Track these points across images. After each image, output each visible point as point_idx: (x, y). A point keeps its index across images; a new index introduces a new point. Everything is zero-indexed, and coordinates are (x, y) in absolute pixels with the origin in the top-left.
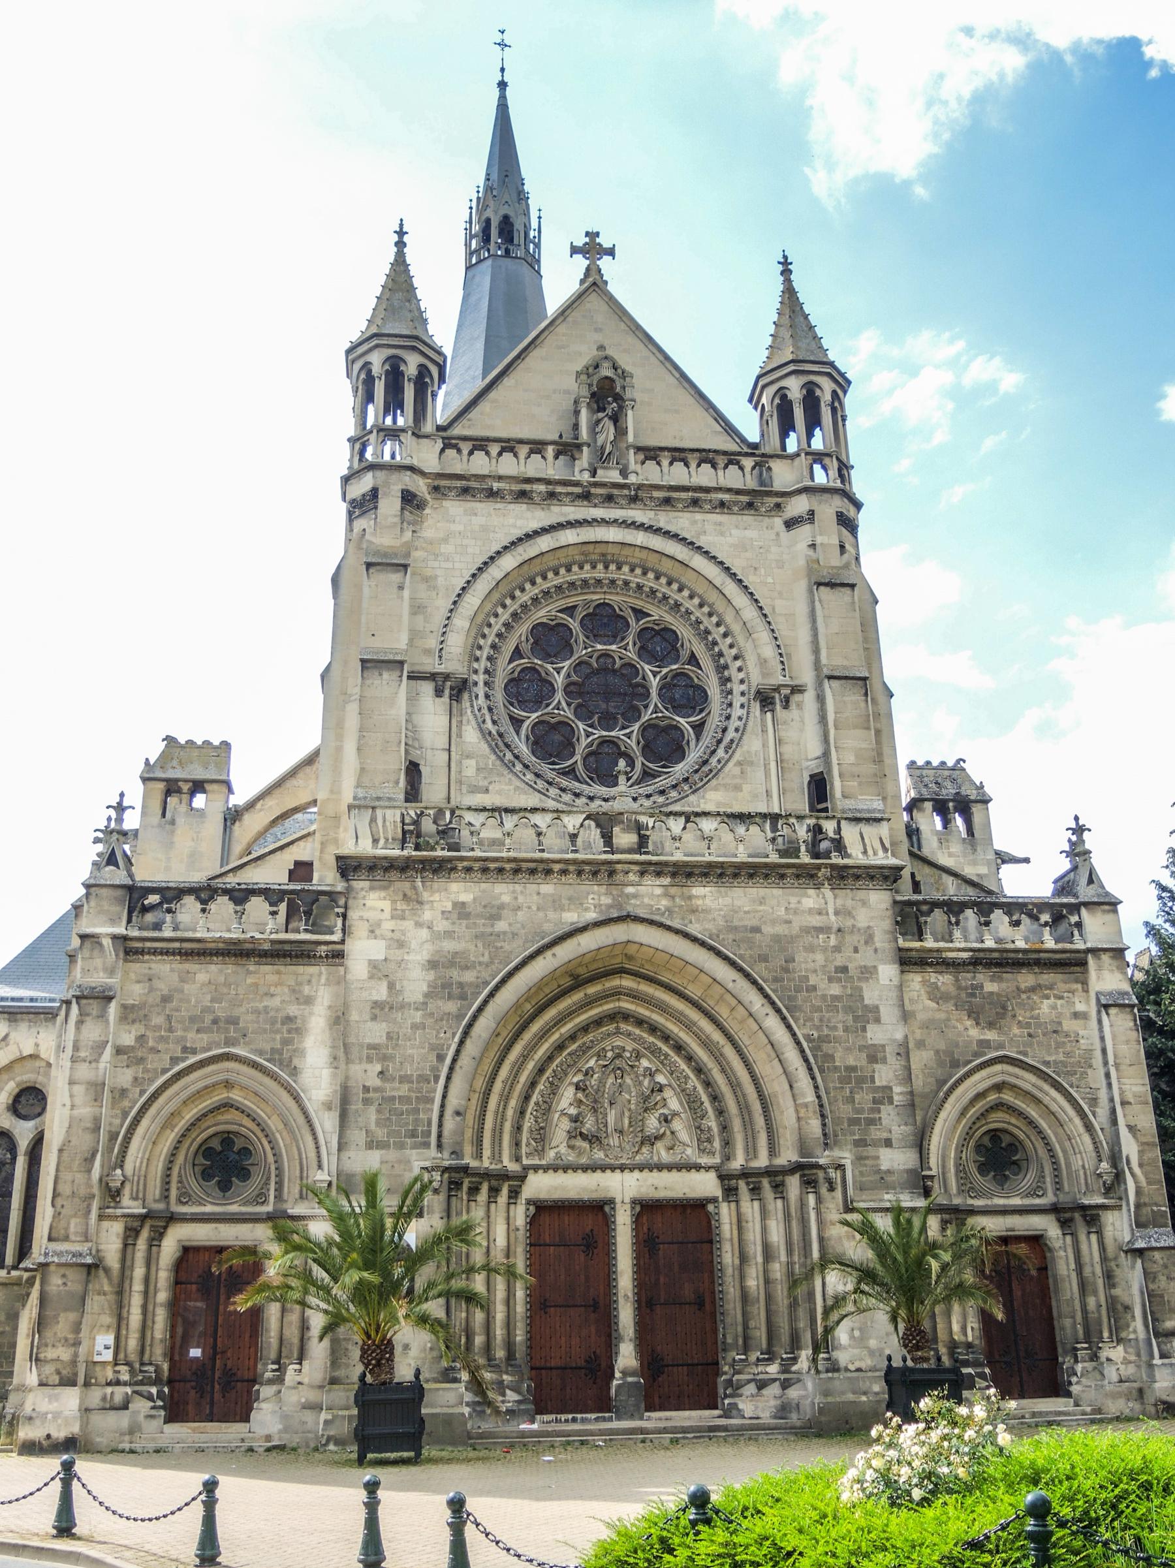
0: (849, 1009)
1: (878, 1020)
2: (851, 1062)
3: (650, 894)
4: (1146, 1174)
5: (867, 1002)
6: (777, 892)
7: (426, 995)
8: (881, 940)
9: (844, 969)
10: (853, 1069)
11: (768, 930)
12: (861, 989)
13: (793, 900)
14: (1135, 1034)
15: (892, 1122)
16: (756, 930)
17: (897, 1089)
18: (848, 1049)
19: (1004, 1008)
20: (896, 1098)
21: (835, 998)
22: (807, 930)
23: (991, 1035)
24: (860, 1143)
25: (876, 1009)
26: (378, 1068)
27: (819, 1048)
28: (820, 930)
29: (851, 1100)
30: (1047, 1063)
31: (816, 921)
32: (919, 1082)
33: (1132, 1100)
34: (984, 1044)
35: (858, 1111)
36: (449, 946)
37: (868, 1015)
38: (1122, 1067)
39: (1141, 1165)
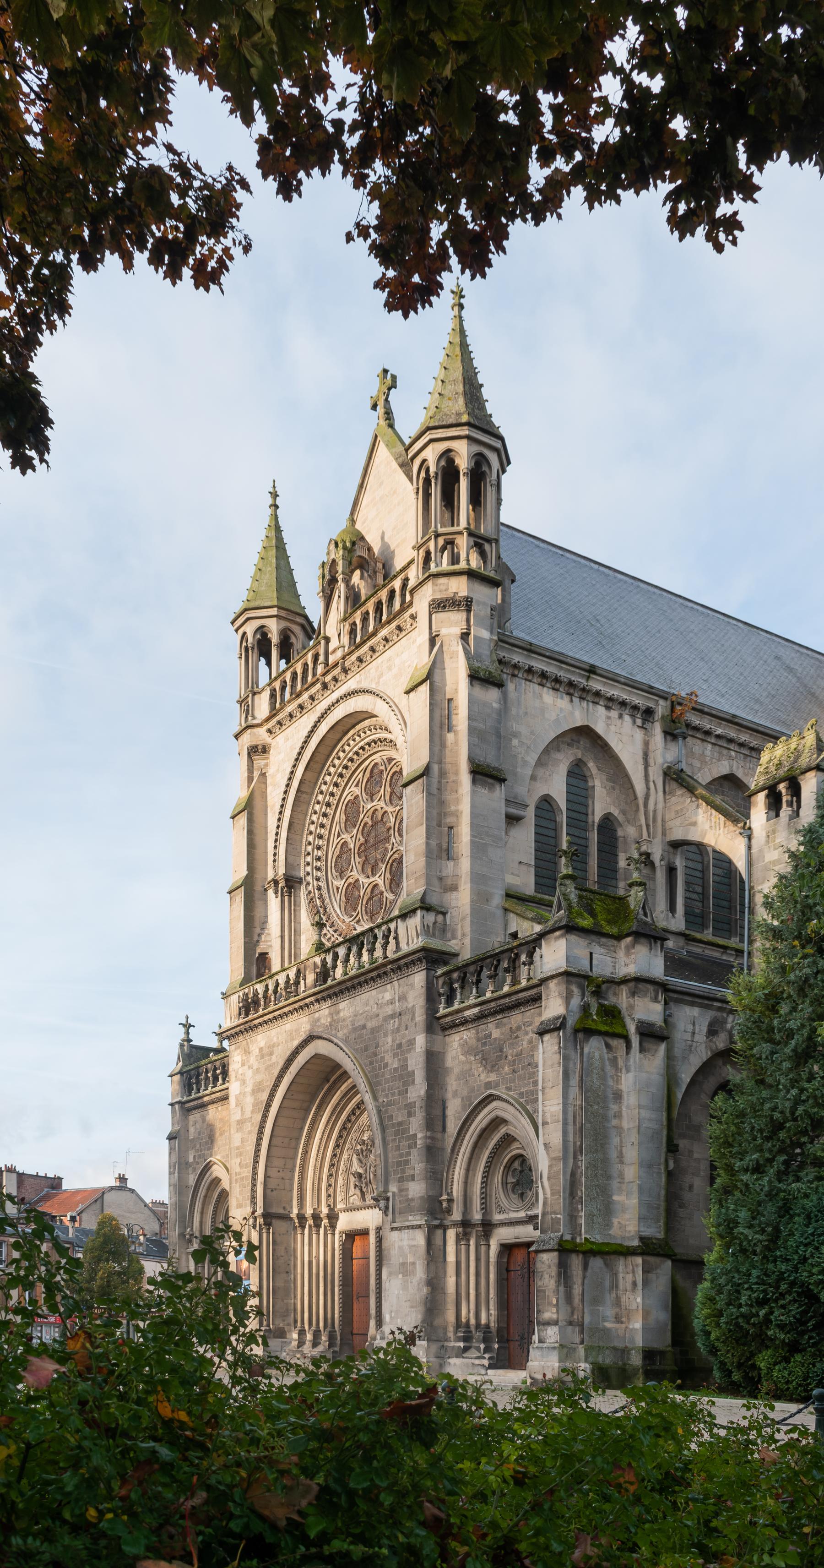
0: (401, 1077)
1: (413, 1082)
2: (400, 1119)
3: (323, 1012)
4: (551, 1186)
5: (410, 1069)
6: (374, 992)
7: (252, 1112)
8: (420, 1016)
9: (400, 1046)
10: (400, 1124)
11: (370, 1025)
12: (406, 1060)
13: (380, 996)
14: (557, 1056)
15: (417, 1165)
16: (364, 1027)
17: (419, 1136)
18: (399, 1109)
19: (501, 1051)
20: (419, 1142)
21: (396, 1070)
22: (387, 1018)
23: (493, 1077)
24: (401, 1180)
25: (413, 1072)
26: (238, 1160)
27: (386, 1111)
28: (392, 1016)
29: (398, 1148)
30: (521, 1095)
31: (389, 1010)
32: (452, 1127)
33: (549, 1121)
34: (488, 1085)
35: (401, 1156)
36: (259, 1078)
37: (407, 1078)
38: (547, 1090)
39: (549, 1178)
